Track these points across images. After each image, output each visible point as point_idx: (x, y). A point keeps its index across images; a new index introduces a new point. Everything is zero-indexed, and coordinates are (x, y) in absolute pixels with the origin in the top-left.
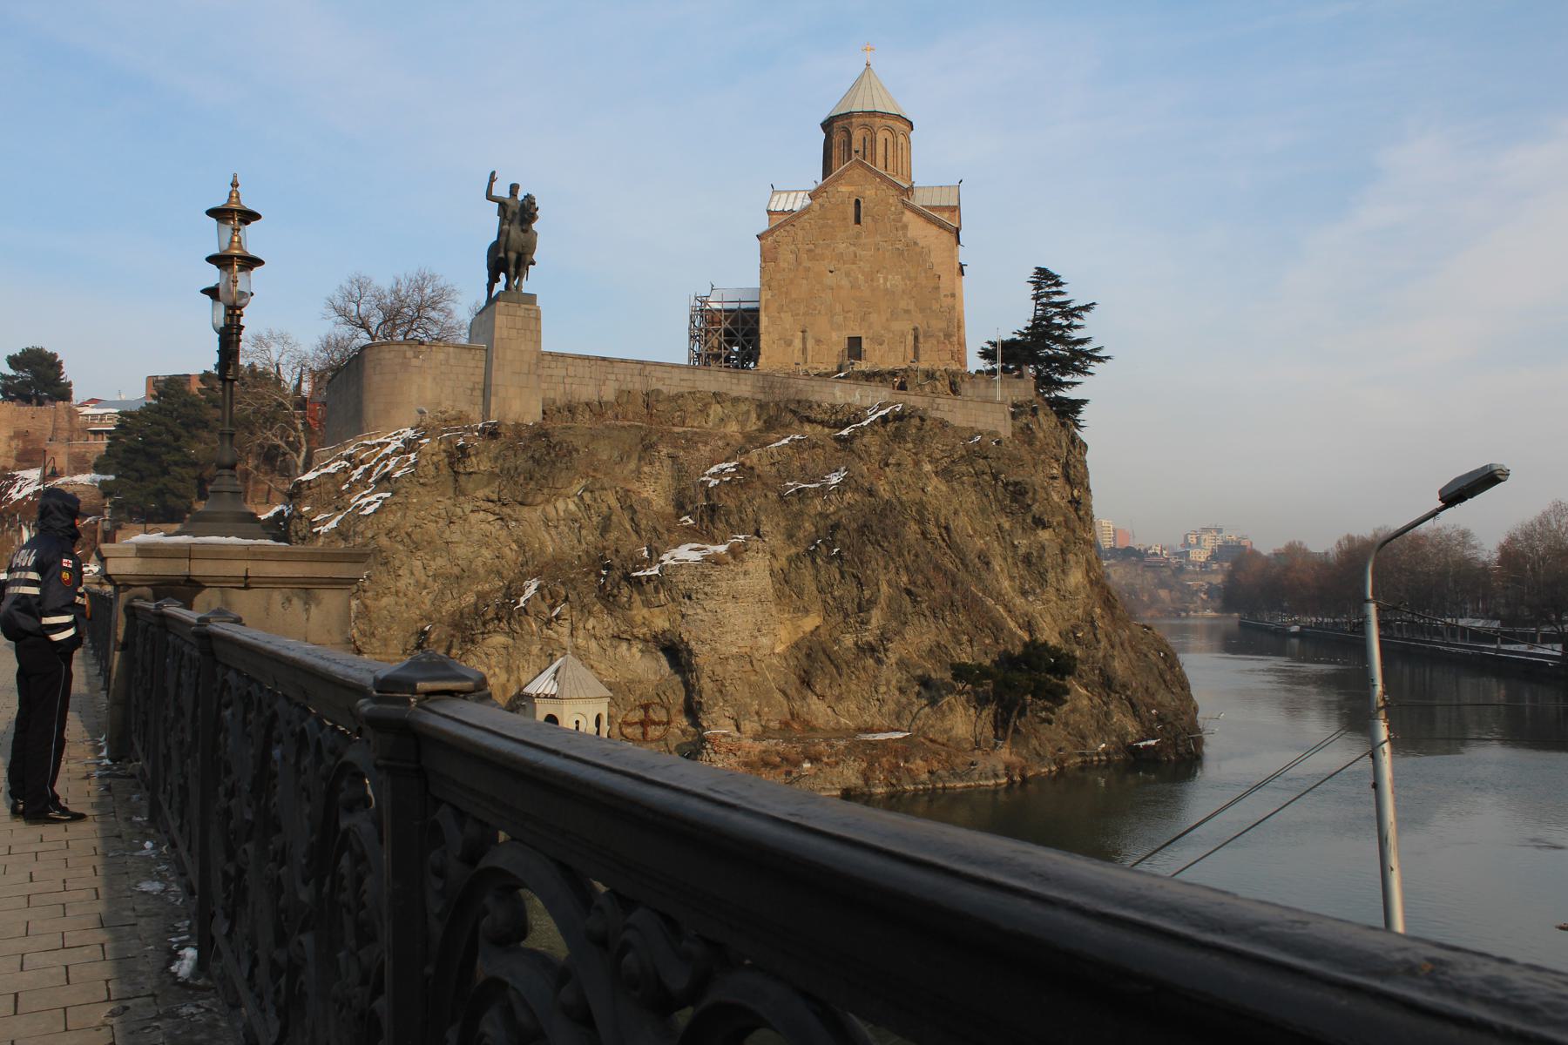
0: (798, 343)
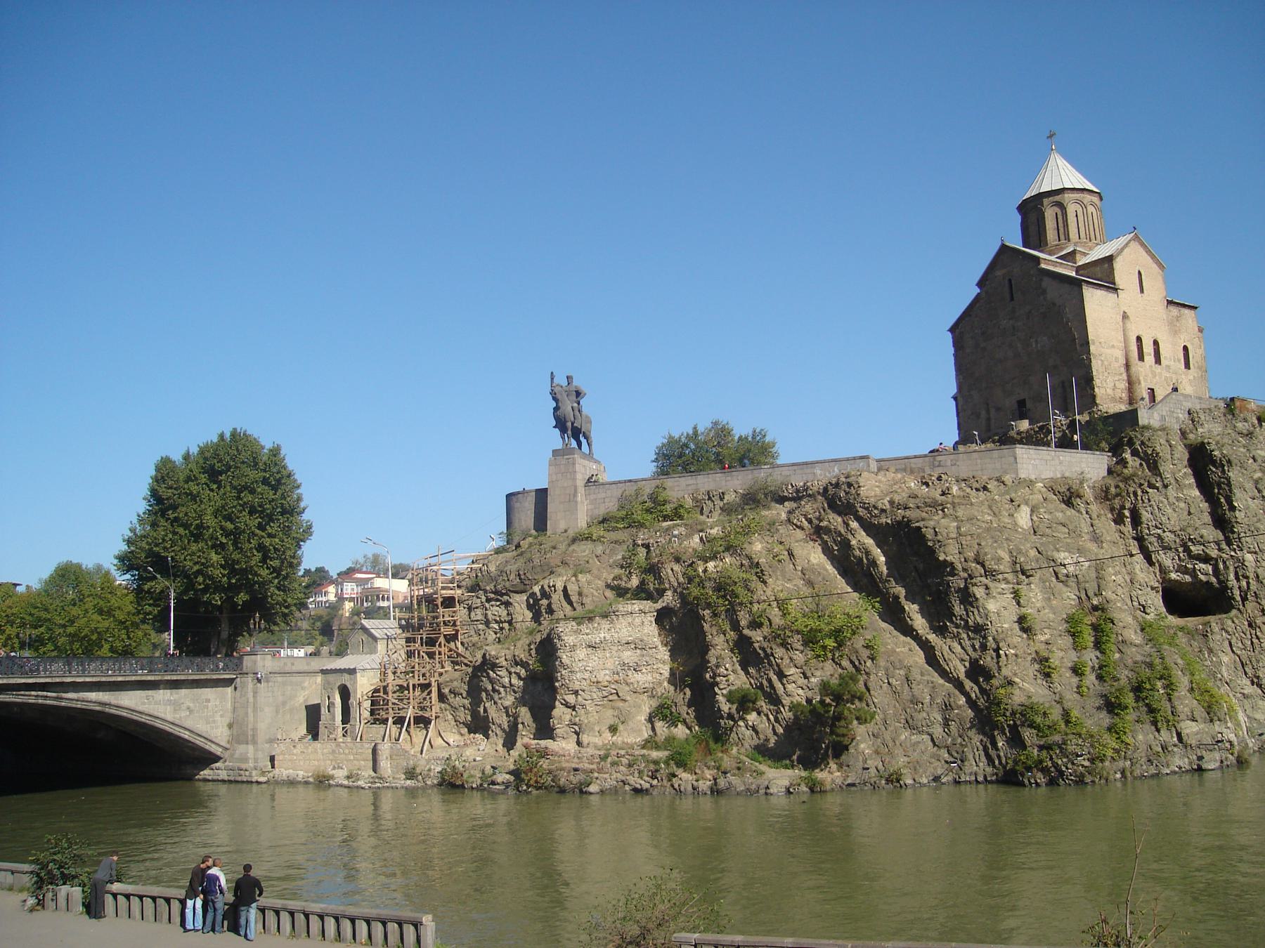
0: (983, 414)
